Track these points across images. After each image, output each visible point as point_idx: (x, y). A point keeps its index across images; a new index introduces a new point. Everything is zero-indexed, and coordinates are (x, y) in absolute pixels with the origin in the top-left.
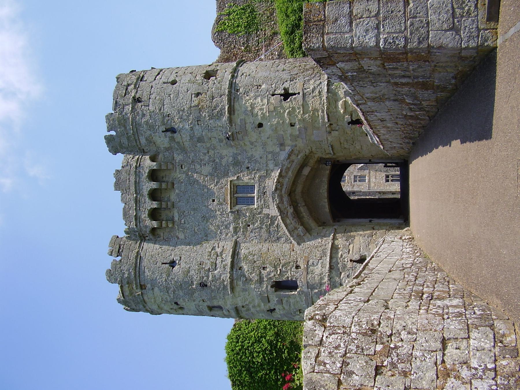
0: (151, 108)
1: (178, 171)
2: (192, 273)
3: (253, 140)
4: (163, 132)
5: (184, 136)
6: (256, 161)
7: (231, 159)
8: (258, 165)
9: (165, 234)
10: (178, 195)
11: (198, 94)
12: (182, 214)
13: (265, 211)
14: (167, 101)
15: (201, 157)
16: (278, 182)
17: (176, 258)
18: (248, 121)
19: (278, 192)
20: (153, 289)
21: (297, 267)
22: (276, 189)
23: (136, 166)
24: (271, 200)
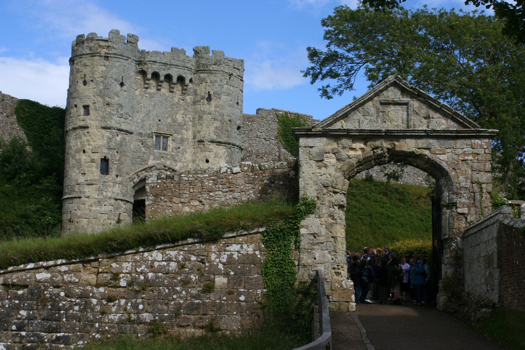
0: (225, 86)
1: (181, 97)
2: (117, 99)
3: (198, 155)
4: (209, 92)
5: (204, 106)
6: (183, 154)
7: (186, 137)
8: (181, 155)
9: (139, 81)
10: (165, 94)
11: (230, 121)
12: (151, 95)
13: (152, 157)
14: (229, 98)
15: (188, 116)
16: (170, 168)
17: (124, 88)
18: (211, 153)
19: (163, 167)
20: (104, 66)
21: (117, 176)
22: (165, 167)
23: (187, 67)
24: (158, 162)
